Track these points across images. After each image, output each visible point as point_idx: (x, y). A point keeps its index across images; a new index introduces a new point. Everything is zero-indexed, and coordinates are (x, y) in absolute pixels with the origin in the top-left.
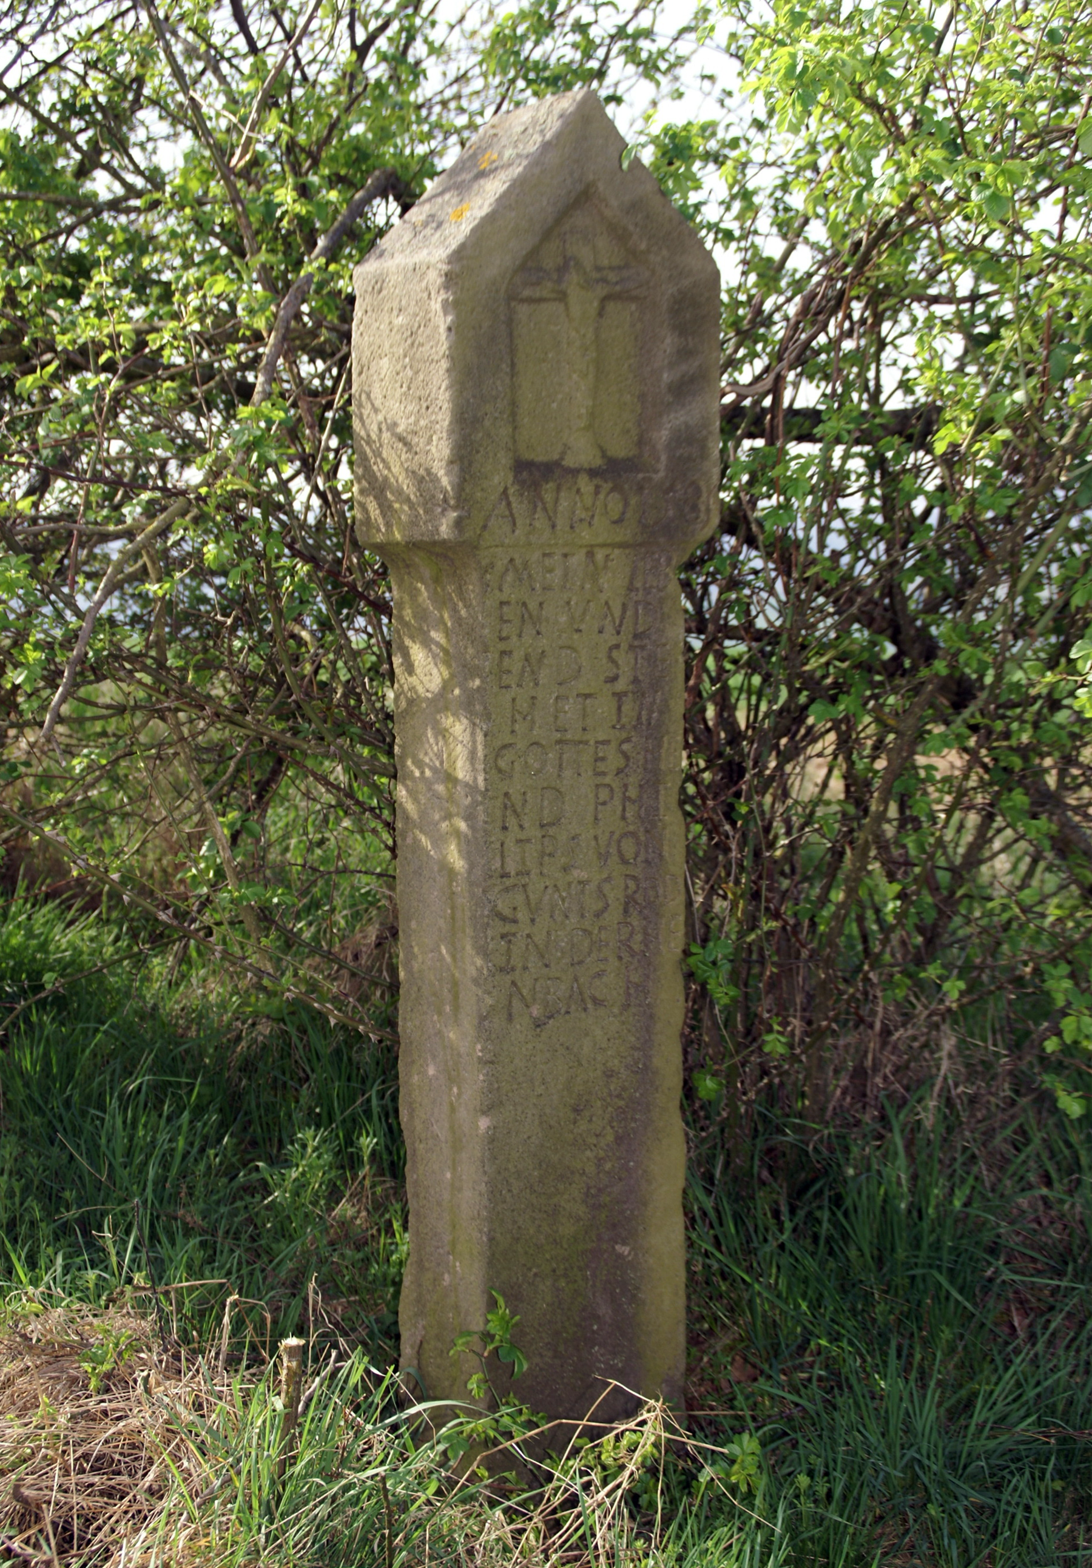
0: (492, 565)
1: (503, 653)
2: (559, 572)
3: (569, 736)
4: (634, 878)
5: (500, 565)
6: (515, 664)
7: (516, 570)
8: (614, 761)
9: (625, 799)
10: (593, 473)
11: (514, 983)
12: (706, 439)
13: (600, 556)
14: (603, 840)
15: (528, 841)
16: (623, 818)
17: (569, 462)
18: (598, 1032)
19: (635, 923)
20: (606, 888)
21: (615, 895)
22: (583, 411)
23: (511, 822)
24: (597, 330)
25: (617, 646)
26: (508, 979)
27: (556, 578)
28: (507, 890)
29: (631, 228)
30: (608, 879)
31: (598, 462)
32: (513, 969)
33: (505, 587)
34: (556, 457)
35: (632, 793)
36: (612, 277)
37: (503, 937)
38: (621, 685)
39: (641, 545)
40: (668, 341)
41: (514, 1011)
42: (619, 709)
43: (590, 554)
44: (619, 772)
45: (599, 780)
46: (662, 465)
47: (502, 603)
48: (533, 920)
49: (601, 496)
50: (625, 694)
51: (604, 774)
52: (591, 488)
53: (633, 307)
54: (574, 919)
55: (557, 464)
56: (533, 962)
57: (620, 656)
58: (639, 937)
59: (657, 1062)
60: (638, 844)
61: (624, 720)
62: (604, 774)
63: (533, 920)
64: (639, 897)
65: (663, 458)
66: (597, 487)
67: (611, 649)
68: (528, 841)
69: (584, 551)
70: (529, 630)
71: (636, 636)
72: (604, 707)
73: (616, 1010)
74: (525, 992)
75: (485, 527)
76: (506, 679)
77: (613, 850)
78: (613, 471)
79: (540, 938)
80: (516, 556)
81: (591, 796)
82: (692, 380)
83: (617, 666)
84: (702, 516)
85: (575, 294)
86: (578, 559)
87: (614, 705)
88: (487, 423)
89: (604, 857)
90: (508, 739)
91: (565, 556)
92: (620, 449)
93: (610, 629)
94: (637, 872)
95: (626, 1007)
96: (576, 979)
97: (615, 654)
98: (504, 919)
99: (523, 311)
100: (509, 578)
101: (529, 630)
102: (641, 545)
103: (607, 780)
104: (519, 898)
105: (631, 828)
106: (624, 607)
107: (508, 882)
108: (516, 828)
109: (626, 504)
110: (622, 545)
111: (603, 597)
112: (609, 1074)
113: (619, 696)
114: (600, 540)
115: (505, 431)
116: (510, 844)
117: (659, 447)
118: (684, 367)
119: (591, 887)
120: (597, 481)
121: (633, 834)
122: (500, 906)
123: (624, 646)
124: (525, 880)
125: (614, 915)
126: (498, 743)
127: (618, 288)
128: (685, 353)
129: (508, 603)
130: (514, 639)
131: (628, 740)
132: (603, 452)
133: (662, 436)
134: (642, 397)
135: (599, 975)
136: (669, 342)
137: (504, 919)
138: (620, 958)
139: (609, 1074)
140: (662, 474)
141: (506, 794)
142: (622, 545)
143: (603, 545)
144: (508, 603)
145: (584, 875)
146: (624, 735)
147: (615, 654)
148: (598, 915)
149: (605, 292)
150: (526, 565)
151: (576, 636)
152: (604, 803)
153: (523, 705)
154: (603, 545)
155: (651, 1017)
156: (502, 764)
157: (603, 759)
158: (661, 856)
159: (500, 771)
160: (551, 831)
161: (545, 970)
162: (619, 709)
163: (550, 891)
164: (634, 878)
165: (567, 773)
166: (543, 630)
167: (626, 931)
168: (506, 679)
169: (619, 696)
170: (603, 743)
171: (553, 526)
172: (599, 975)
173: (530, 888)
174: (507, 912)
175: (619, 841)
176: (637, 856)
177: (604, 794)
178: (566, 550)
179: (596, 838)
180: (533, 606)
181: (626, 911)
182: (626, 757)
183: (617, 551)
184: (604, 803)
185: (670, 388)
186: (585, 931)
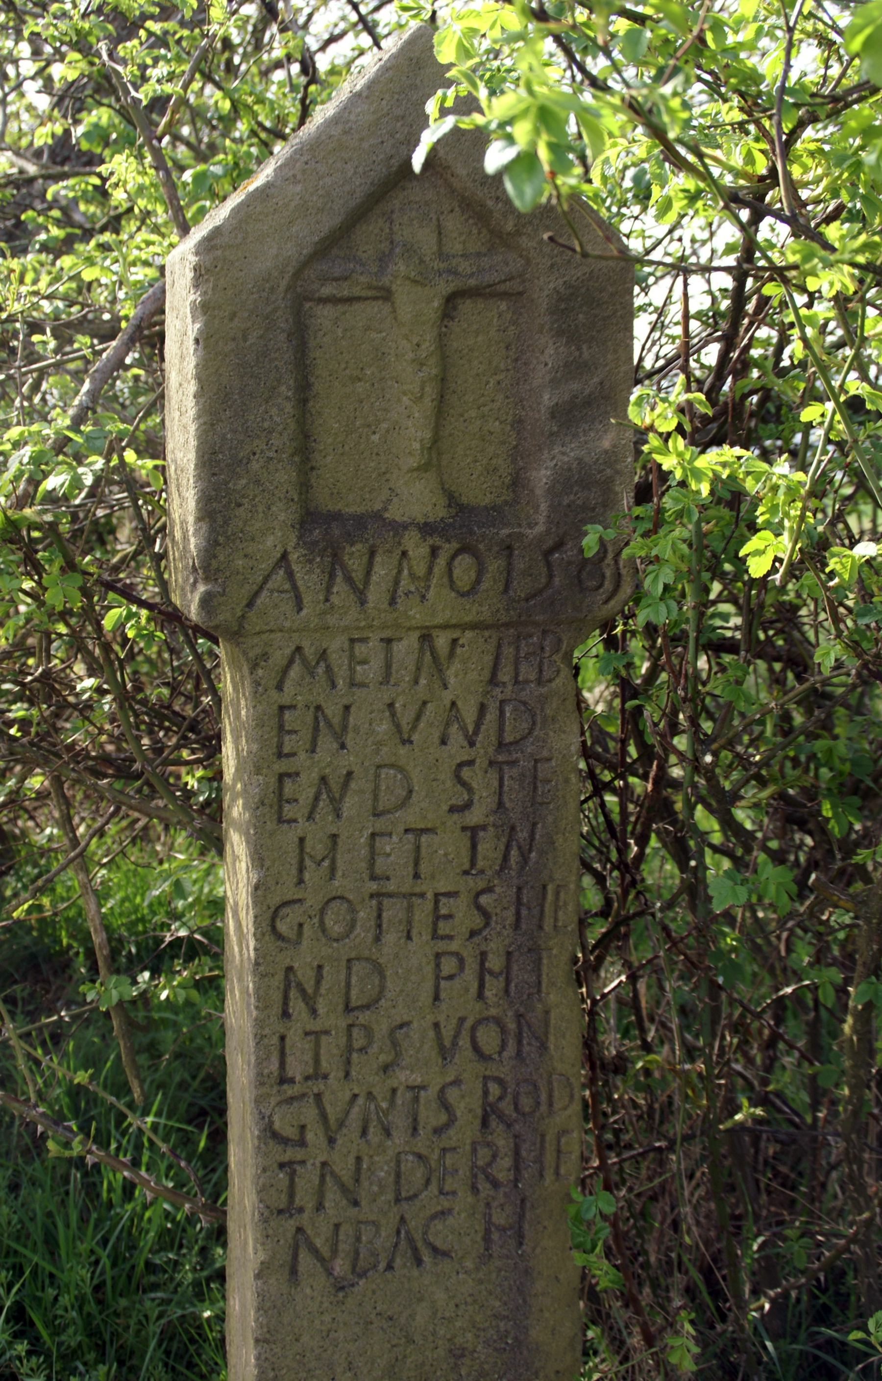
0: (265, 656)
1: (281, 777)
2: (376, 664)
3: (391, 887)
4: (500, 1082)
5: (279, 657)
6: (303, 789)
7: (305, 662)
8: (464, 916)
9: (483, 971)
10: (426, 529)
11: (299, 1230)
12: (610, 481)
13: (442, 641)
14: (447, 1033)
15: (327, 1032)
16: (480, 995)
17: (394, 513)
18: (440, 1296)
19: (501, 1143)
20: (453, 1095)
21: (466, 1104)
22: (417, 446)
23: (297, 1006)
24: (442, 341)
25: (471, 763)
26: (291, 1225)
27: (371, 671)
28: (291, 1100)
29: (490, 203)
30: (457, 1082)
31: (439, 512)
32: (301, 1210)
33: (288, 685)
34: (378, 506)
35: (495, 963)
36: (464, 267)
37: (282, 1166)
38: (475, 817)
39: (507, 625)
40: (550, 351)
41: (301, 1269)
42: (474, 847)
43: (426, 638)
44: (473, 934)
45: (442, 946)
46: (542, 519)
47: (282, 708)
48: (331, 1141)
49: (441, 562)
50: (484, 828)
51: (450, 938)
52: (424, 550)
53: (503, 306)
54: (399, 1138)
55: (378, 516)
56: (332, 1196)
57: (473, 776)
58: (506, 1162)
59: (536, 1334)
60: (503, 1030)
61: (480, 864)
62: (450, 938)
63: (331, 1141)
64: (506, 1107)
65: (543, 507)
66: (434, 552)
67: (460, 765)
68: (327, 1032)
69: (416, 634)
70: (327, 743)
71: (501, 745)
72: (447, 846)
73: (469, 1264)
74: (318, 1242)
75: (250, 604)
76: (289, 811)
77: (464, 1042)
78: (461, 527)
79: (343, 1168)
80: (306, 644)
81: (429, 969)
82: (588, 403)
83: (470, 790)
84: (608, 585)
85: (403, 294)
86: (406, 647)
87: (465, 842)
88: (255, 466)
89: (445, 1053)
90: (291, 893)
91: (389, 641)
92: (479, 491)
93: (456, 736)
94: (504, 1071)
95: (486, 1257)
96: (402, 1219)
97: (466, 773)
98: (284, 1141)
99: (325, 314)
100: (295, 672)
101: (327, 743)
102: (507, 625)
103: (454, 946)
104: (310, 1113)
105: (493, 1012)
106: (482, 709)
107: (290, 1091)
108: (305, 1015)
109: (480, 573)
110: (474, 626)
111: (447, 696)
112: (458, 1354)
113: (473, 832)
114: (439, 621)
115: (284, 477)
116: (294, 1037)
117: (539, 492)
118: (575, 386)
119: (432, 1092)
120: (437, 540)
121: (498, 1021)
122: (277, 1126)
123: (481, 762)
124: (318, 1086)
125: (465, 1130)
126: (275, 900)
127: (472, 282)
128: (575, 368)
129: (292, 707)
130: (303, 756)
131: (489, 890)
132: (451, 498)
133: (541, 476)
134: (518, 423)
135: (443, 1214)
136: (550, 353)
137: (284, 1141)
138: (475, 1190)
139: (458, 1354)
140: (540, 528)
141: (290, 969)
142: (474, 626)
143: (445, 627)
144: (292, 707)
145: (416, 1079)
146: (481, 885)
147: (466, 773)
148: (438, 1131)
149: (451, 288)
150: (323, 655)
151: (402, 751)
152: (450, 977)
153: (316, 846)
154: (445, 627)
155: (527, 1272)
156: (282, 927)
157: (450, 916)
158: (543, 1047)
159: (279, 937)
160: (363, 1017)
161: (353, 1211)
162: (474, 847)
163: (360, 1101)
164: (500, 1082)
165: (390, 938)
166: (349, 742)
167: (484, 1154)
168: (289, 811)
169: (473, 832)
170: (448, 895)
171: (363, 602)
172: (443, 1214)
173: (326, 1099)
174: (290, 1132)
175: (473, 1029)
176: (503, 1046)
177: (448, 966)
178: (387, 634)
179: (436, 1025)
180: (333, 711)
181: (485, 1123)
182: (486, 915)
183: (469, 634)
184: (450, 977)
185: (553, 414)
186: (420, 1156)
